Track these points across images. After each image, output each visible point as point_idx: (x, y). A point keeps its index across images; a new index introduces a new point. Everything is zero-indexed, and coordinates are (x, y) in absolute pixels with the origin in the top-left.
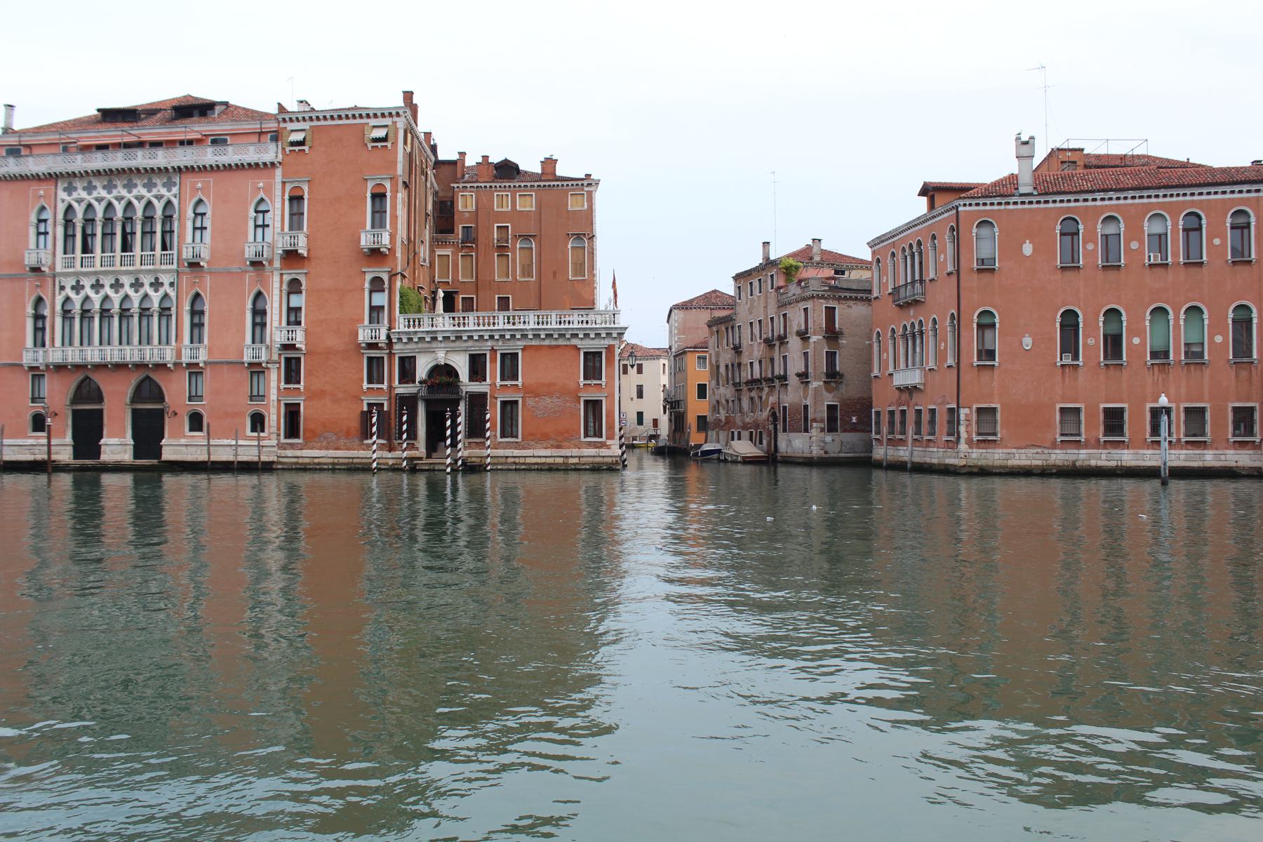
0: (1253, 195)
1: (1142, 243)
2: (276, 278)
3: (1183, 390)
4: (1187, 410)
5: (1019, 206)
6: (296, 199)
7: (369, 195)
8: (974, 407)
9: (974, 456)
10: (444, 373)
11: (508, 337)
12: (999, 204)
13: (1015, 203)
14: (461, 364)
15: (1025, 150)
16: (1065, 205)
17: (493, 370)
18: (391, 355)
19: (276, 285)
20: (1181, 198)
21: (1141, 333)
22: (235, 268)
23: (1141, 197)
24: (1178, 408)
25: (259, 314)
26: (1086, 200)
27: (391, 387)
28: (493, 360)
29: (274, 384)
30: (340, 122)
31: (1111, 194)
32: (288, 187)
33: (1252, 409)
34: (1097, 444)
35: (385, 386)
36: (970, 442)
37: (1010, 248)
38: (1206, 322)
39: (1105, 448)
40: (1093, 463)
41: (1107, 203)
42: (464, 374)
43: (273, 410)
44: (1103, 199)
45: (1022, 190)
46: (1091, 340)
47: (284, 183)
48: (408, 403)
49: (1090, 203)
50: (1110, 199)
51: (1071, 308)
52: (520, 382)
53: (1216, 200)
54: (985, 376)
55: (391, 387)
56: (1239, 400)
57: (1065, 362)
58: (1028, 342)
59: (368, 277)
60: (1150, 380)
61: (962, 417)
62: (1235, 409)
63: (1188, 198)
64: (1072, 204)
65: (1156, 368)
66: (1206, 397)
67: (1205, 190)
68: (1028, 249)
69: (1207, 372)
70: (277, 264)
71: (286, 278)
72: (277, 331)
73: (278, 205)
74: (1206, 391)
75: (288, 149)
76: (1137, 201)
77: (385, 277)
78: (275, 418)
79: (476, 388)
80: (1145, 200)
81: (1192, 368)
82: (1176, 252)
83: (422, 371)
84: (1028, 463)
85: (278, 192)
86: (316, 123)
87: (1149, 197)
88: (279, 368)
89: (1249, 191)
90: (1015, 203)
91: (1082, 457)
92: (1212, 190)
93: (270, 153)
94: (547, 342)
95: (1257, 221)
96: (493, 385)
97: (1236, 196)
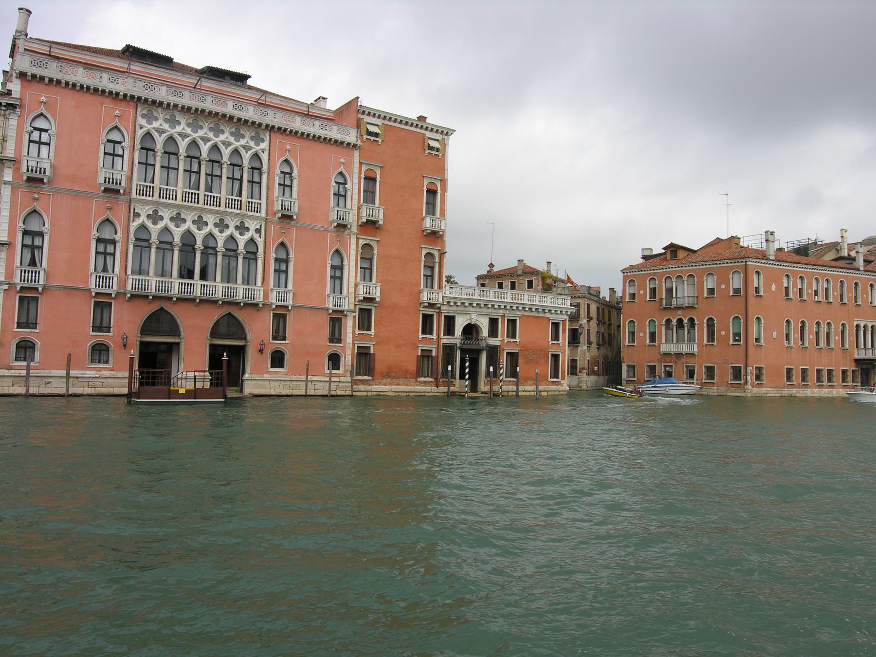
2: (353, 241)
6: (370, 180)
7: (425, 189)
10: (470, 330)
11: (496, 307)
14: (484, 324)
18: (439, 313)
19: (353, 247)
22: (319, 226)
25: (338, 269)
27: (439, 338)
29: (350, 330)
30: (406, 127)
32: (364, 168)
35: (434, 336)
37: (767, 287)
42: (485, 332)
43: (349, 352)
46: (795, 335)
47: (361, 163)
48: (449, 351)
52: (517, 339)
55: (439, 338)
58: (775, 334)
59: (424, 252)
61: (749, 371)
68: (774, 287)
70: (354, 229)
71: (362, 242)
73: (356, 181)
75: (365, 137)
77: (436, 254)
78: (348, 359)
79: (493, 342)
82: (821, 297)
85: (356, 170)
86: (386, 122)
88: (355, 317)
93: (351, 137)
94: (532, 314)
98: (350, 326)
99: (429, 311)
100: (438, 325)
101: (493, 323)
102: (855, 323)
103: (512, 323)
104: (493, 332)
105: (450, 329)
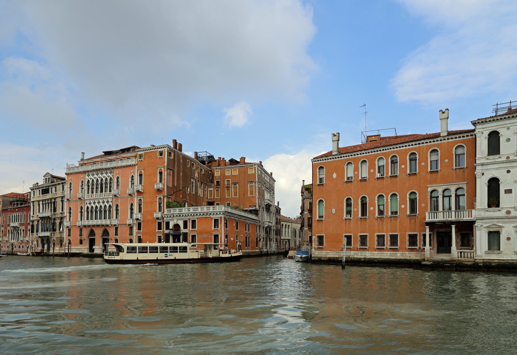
0: (418, 146)
1: (375, 170)
3: (389, 228)
4: (391, 236)
5: (332, 160)
8: (317, 235)
9: (316, 253)
10: (177, 226)
12: (325, 160)
13: (331, 159)
15: (336, 138)
16: (348, 157)
17: (190, 224)
20: (389, 150)
21: (374, 206)
23: (374, 151)
24: (403, 237)
26: (355, 155)
28: (190, 222)
31: (363, 152)
33: (416, 235)
34: (357, 250)
36: (315, 248)
38: (398, 200)
39: (360, 251)
40: (356, 256)
41: (362, 155)
44: (361, 154)
45: (333, 154)
49: (356, 156)
50: (363, 153)
51: (362, 196)
53: (403, 150)
54: (320, 223)
56: (411, 231)
57: (347, 218)
60: (376, 224)
62: (410, 235)
63: (392, 150)
64: (350, 157)
65: (379, 219)
66: (398, 230)
67: (398, 146)
68: (335, 176)
69: (398, 220)
72: (137, 215)
74: (398, 228)
76: (373, 153)
80: (376, 153)
81: (393, 218)
83: (171, 227)
84: (334, 256)
87: (377, 151)
89: (416, 144)
90: (331, 159)
91: (352, 254)
92: (401, 145)
95: (419, 156)
96: (189, 230)
97: (411, 147)
98: (135, 229)
99: (159, 221)
100: (164, 226)
101: (185, 223)
102: (430, 190)
103: (194, 222)
104: (185, 227)
105: (168, 227)
